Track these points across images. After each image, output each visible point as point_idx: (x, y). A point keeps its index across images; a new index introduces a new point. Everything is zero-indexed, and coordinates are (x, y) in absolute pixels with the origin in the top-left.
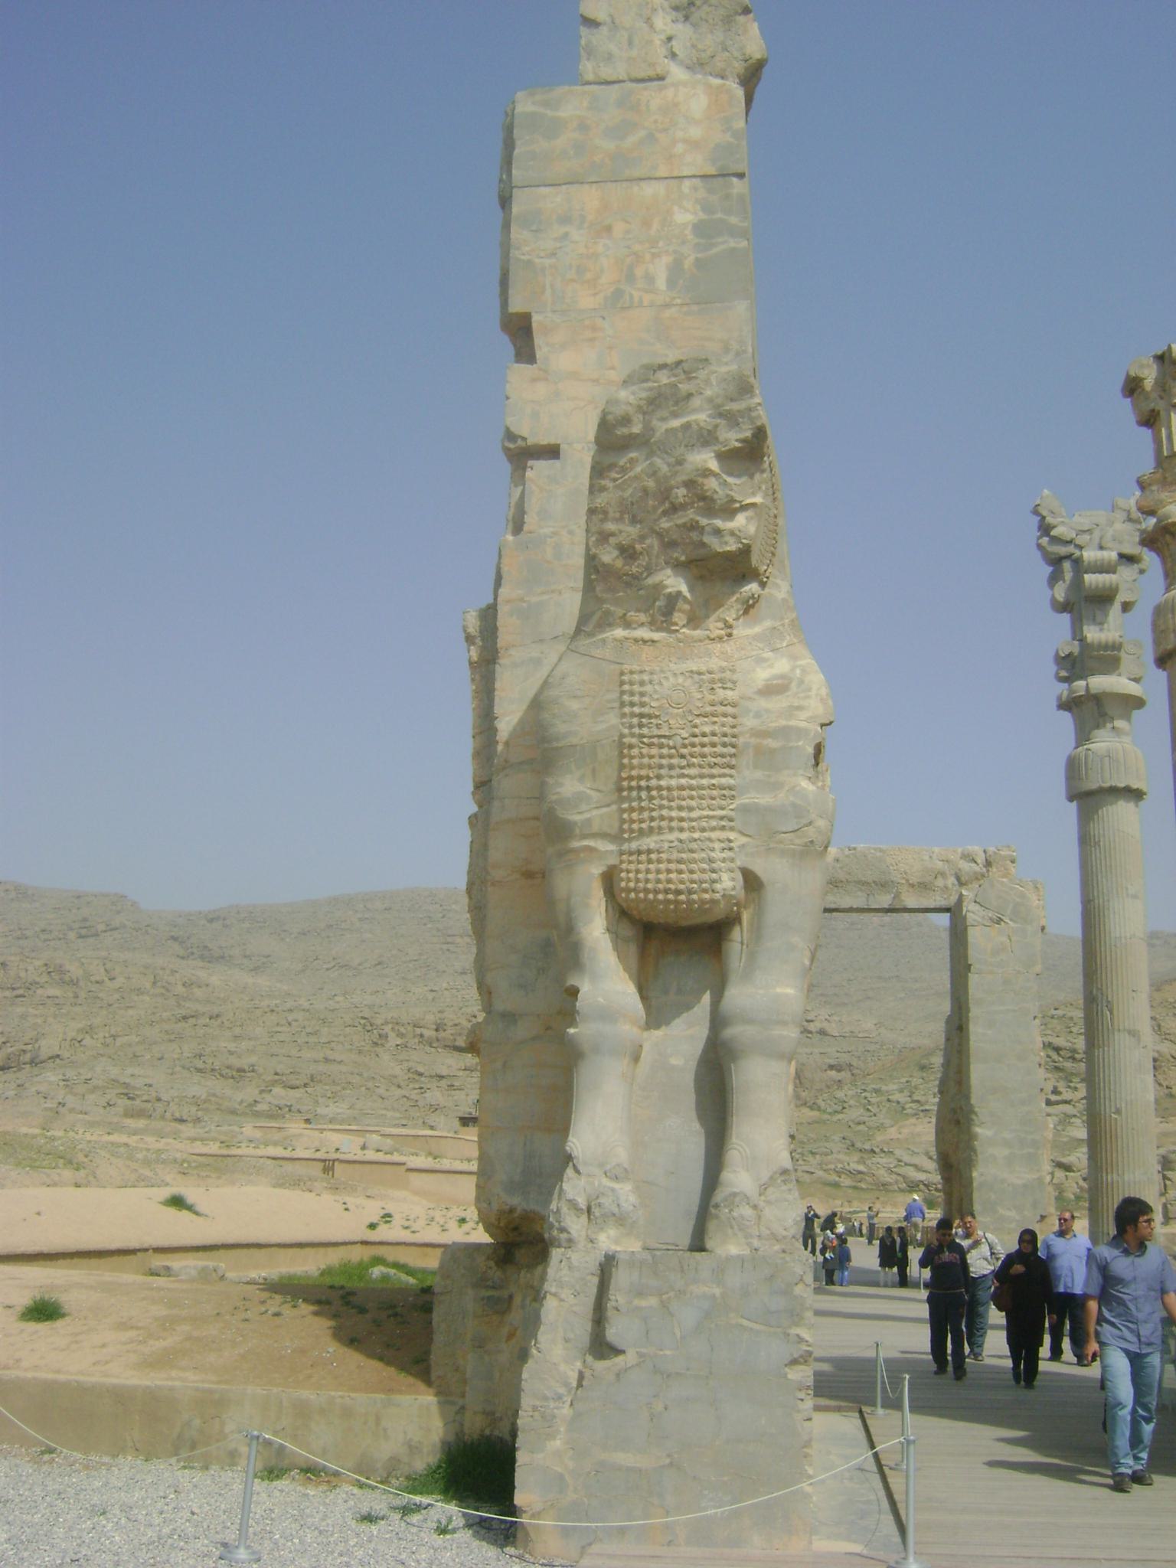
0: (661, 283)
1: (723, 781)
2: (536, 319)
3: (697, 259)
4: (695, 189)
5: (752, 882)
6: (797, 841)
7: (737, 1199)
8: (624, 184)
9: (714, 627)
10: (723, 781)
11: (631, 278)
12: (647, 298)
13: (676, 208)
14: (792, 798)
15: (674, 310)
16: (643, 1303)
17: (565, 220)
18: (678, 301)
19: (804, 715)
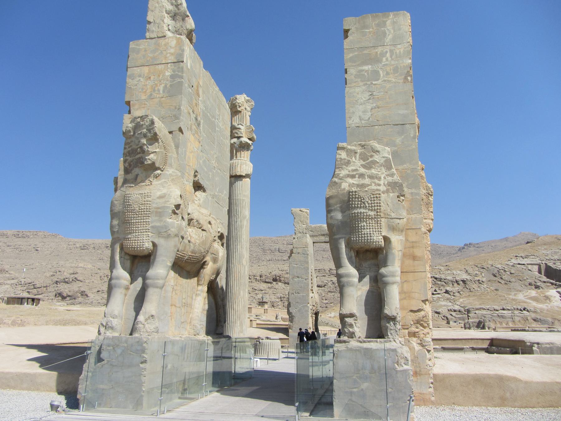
0: (161, 92)
1: (147, 220)
2: (131, 102)
4: (171, 66)
5: (154, 245)
6: (166, 234)
7: (139, 323)
8: (154, 66)
9: (147, 182)
10: (147, 220)
11: (154, 90)
12: (158, 96)
13: (166, 72)
14: (164, 224)
15: (164, 98)
16: (109, 348)
17: (140, 76)
18: (165, 96)
19: (169, 203)
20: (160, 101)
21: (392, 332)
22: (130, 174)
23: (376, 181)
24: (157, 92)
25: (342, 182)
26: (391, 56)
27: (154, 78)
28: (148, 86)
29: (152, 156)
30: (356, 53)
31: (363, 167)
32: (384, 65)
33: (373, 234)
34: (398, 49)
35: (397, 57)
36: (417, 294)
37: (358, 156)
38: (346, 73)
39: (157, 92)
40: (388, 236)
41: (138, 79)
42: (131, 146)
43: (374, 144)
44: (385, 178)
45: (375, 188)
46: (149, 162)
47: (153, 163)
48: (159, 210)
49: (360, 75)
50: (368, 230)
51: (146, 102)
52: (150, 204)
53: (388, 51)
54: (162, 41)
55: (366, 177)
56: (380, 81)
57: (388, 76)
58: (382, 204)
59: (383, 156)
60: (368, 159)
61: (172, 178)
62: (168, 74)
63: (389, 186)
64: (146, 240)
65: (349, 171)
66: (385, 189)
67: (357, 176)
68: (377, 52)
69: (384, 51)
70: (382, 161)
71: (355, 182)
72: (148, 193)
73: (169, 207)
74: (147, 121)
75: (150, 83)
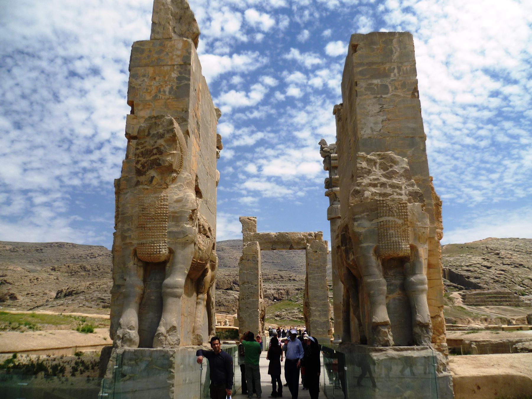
0: (167, 93)
2: (135, 102)
3: (177, 87)
4: (178, 68)
11: (160, 91)
12: (163, 97)
13: (172, 73)
14: (182, 229)
15: (170, 100)
17: (144, 76)
19: (186, 208)
20: (165, 102)
21: (426, 339)
22: (144, 176)
24: (162, 93)
26: (399, 72)
27: (160, 79)
28: (153, 87)
29: (169, 158)
30: (365, 67)
32: (393, 80)
33: (402, 242)
34: (405, 66)
35: (404, 74)
36: (433, 301)
37: (378, 166)
38: (357, 85)
39: (162, 93)
40: (415, 244)
41: (142, 79)
42: (145, 146)
43: (392, 154)
45: (397, 197)
46: (167, 164)
47: (171, 165)
48: (176, 215)
49: (370, 87)
50: (397, 239)
51: (151, 103)
52: (167, 208)
53: (396, 67)
54: (168, 44)
55: (388, 186)
56: (389, 95)
57: (397, 91)
58: (409, 213)
59: (403, 166)
60: (388, 169)
61: (187, 181)
62: (174, 75)
63: (410, 195)
64: (163, 246)
65: (371, 180)
66: (407, 198)
67: (379, 185)
68: (385, 68)
69: (392, 67)
70: (402, 171)
71: (377, 191)
72: (164, 196)
73: (187, 211)
74: (163, 121)
75: (155, 84)
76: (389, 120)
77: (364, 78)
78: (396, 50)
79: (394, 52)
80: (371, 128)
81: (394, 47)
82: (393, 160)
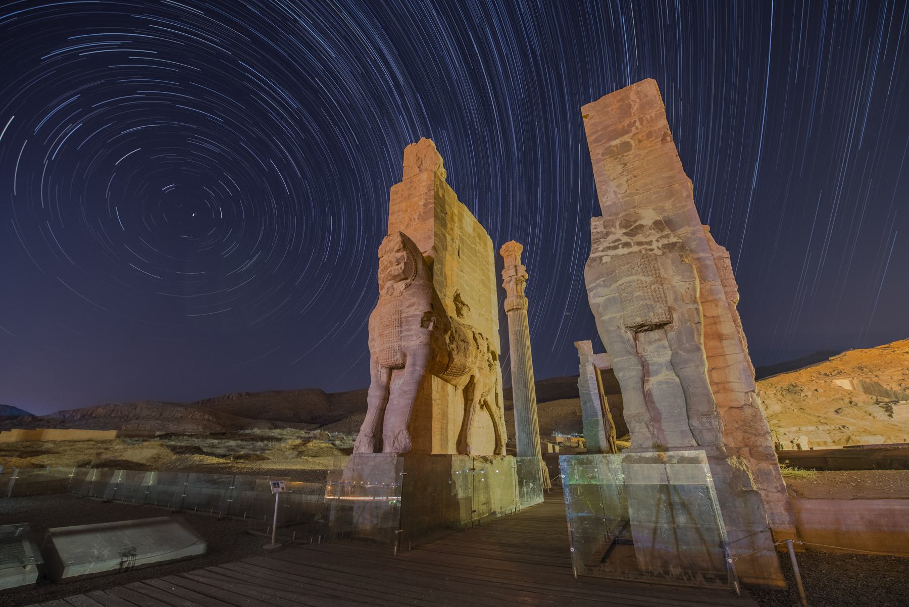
0: (416, 220)
12: (414, 223)
23: (646, 246)
25: (603, 256)
26: (641, 124)
30: (600, 133)
31: (626, 236)
41: (398, 214)
44: (657, 241)
53: (637, 119)
55: (632, 244)
56: (632, 151)
62: (421, 203)
67: (620, 246)
69: (632, 121)
73: (419, 315)
76: (635, 177)
77: (600, 144)
78: (635, 102)
79: (633, 105)
80: (614, 191)
81: (633, 101)
82: (637, 213)
